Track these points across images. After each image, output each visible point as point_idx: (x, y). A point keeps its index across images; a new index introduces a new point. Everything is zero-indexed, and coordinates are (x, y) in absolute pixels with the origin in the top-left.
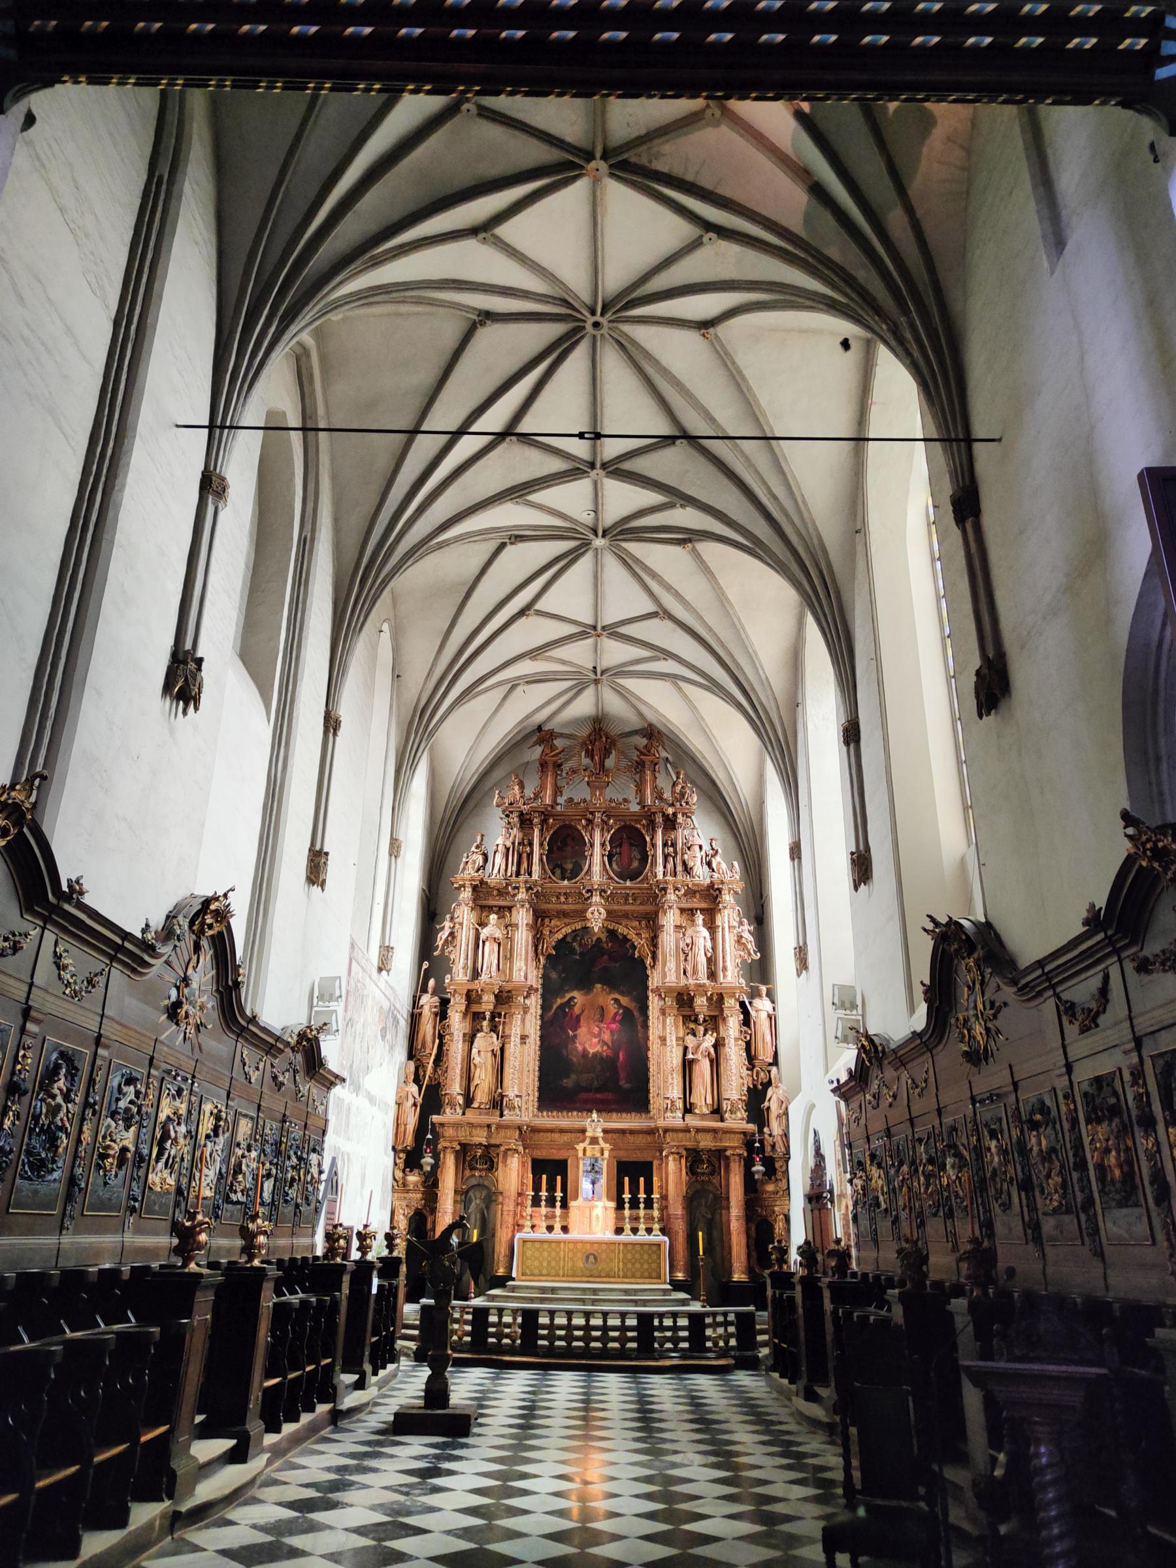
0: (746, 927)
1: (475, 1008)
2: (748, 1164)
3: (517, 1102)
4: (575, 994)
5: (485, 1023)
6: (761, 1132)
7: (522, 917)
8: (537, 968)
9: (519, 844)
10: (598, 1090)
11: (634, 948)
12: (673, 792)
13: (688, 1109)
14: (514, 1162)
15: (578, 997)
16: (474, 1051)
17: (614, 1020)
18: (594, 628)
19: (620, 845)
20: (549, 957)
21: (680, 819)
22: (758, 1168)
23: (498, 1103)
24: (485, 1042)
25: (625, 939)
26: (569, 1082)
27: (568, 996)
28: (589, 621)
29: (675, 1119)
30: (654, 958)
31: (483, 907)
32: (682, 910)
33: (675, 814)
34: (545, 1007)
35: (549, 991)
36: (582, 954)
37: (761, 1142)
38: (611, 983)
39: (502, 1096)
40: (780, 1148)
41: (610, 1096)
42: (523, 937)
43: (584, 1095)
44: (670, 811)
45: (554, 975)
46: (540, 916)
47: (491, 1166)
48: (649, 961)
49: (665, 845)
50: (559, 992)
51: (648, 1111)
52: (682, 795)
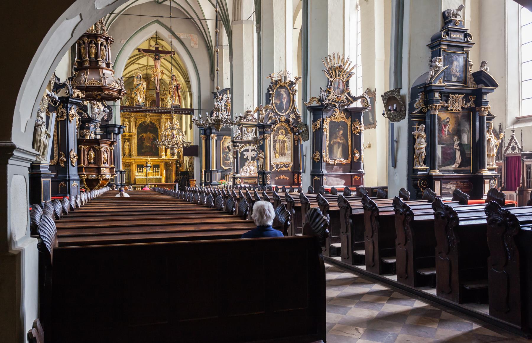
0: (178, 122)
1: (124, 137)
2: (177, 164)
3: (134, 155)
4: (144, 134)
5: (127, 140)
6: (179, 159)
7: (133, 119)
8: (136, 129)
9: (131, 104)
10: (149, 152)
11: (156, 125)
12: (164, 93)
13: (166, 156)
14: (134, 165)
15: (144, 135)
16: (125, 146)
17: (152, 139)
18: (147, 66)
19: (152, 104)
20: (138, 127)
21: (165, 99)
22: (178, 165)
23: (130, 155)
24: (127, 144)
25: (154, 123)
26: (143, 151)
27: (142, 135)
28: (146, 64)
29: (163, 157)
30: (160, 127)
31: (124, 117)
32: (165, 118)
33: (164, 98)
34: (138, 137)
35: (138, 134)
36: (145, 126)
37: (179, 161)
38: (151, 132)
39: (131, 154)
40: (182, 162)
41: (151, 153)
42: (133, 123)
43: (146, 153)
44: (163, 98)
45: (139, 130)
46: (136, 119)
47: (129, 165)
48: (158, 128)
49: (162, 105)
50: (141, 134)
51: (158, 156)
52: (165, 94)
